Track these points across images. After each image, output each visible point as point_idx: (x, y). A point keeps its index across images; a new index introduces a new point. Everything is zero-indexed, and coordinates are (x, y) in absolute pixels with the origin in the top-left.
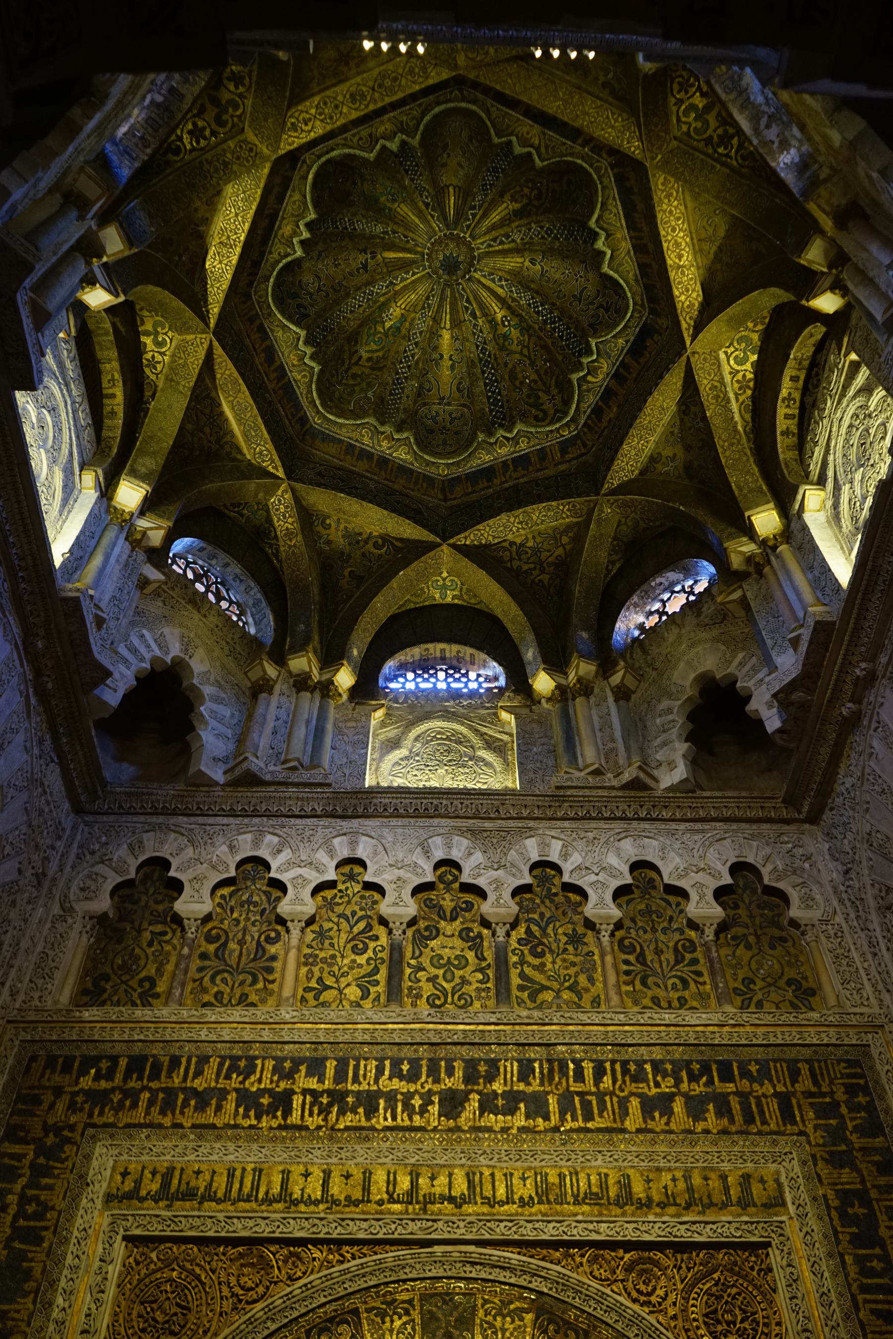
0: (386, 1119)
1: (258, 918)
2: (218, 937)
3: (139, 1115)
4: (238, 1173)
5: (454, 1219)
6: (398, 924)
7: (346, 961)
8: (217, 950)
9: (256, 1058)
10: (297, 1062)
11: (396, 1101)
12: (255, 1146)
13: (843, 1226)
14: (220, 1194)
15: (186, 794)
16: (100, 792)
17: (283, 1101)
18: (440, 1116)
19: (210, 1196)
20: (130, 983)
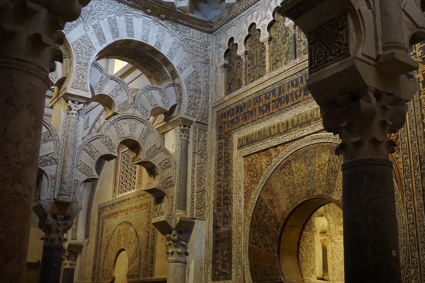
0: (291, 102)
1: (259, 45)
2: (251, 57)
3: (240, 124)
4: (260, 132)
5: (308, 128)
6: (291, 27)
7: (282, 49)
8: (251, 62)
9: (261, 96)
10: (269, 93)
11: (293, 94)
12: (263, 123)
13: (423, 88)
14: (258, 140)
15: (230, 11)
16: (211, 24)
17: (268, 106)
18: (304, 95)
19: (256, 141)
20: (235, 83)
